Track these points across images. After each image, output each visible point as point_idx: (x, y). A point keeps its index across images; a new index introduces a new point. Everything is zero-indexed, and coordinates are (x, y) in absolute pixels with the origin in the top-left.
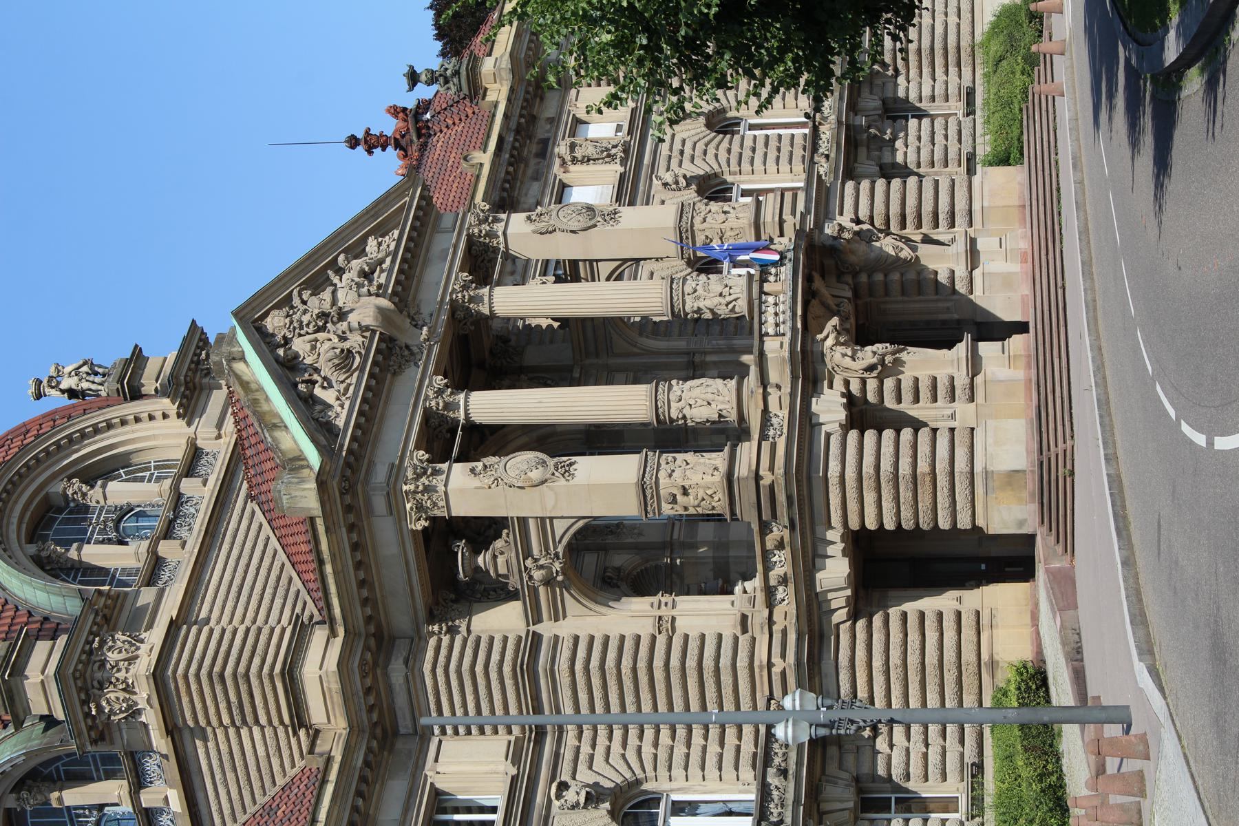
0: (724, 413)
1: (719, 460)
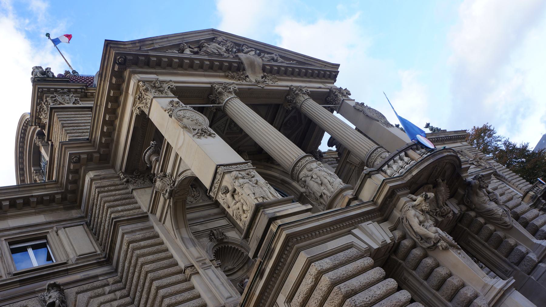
0: (325, 197)
1: (270, 193)
